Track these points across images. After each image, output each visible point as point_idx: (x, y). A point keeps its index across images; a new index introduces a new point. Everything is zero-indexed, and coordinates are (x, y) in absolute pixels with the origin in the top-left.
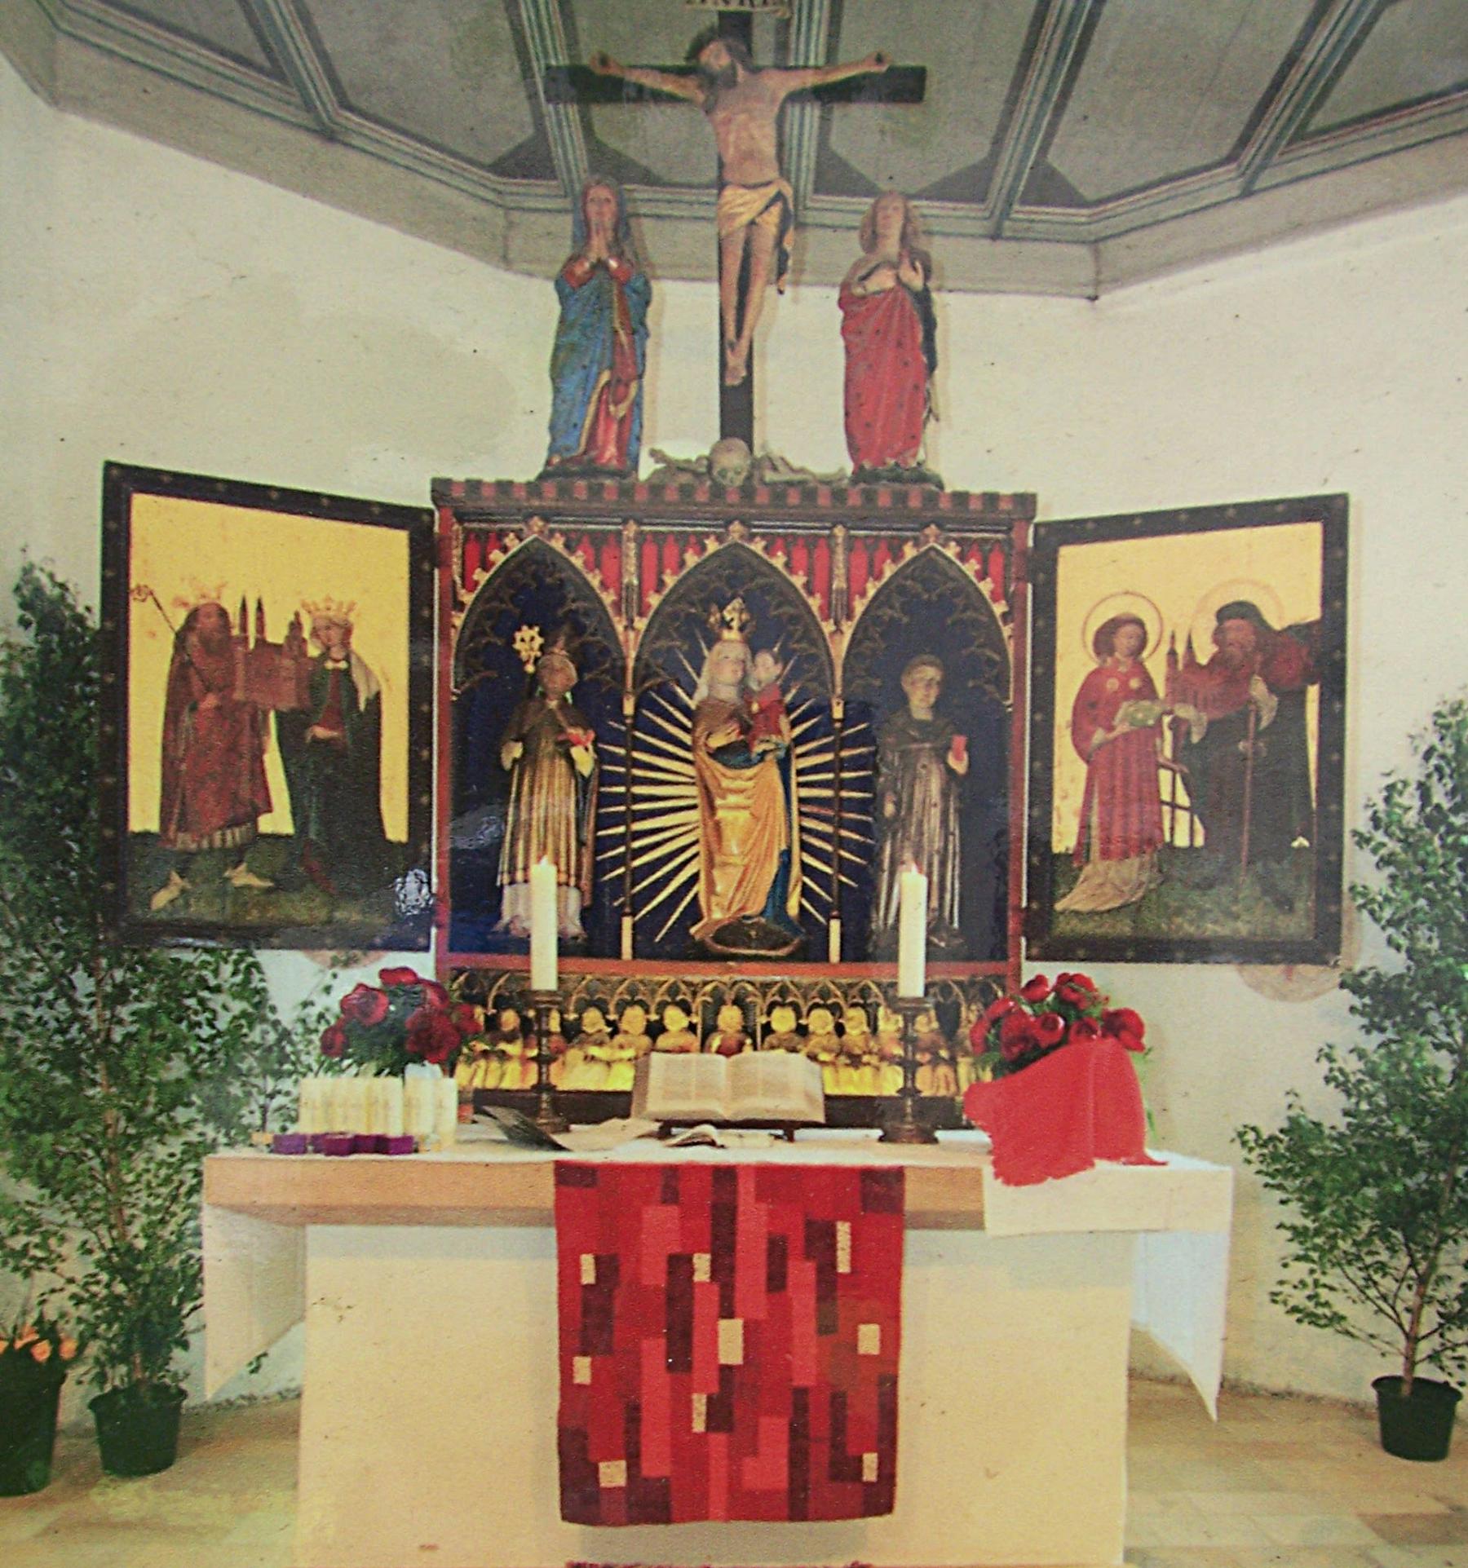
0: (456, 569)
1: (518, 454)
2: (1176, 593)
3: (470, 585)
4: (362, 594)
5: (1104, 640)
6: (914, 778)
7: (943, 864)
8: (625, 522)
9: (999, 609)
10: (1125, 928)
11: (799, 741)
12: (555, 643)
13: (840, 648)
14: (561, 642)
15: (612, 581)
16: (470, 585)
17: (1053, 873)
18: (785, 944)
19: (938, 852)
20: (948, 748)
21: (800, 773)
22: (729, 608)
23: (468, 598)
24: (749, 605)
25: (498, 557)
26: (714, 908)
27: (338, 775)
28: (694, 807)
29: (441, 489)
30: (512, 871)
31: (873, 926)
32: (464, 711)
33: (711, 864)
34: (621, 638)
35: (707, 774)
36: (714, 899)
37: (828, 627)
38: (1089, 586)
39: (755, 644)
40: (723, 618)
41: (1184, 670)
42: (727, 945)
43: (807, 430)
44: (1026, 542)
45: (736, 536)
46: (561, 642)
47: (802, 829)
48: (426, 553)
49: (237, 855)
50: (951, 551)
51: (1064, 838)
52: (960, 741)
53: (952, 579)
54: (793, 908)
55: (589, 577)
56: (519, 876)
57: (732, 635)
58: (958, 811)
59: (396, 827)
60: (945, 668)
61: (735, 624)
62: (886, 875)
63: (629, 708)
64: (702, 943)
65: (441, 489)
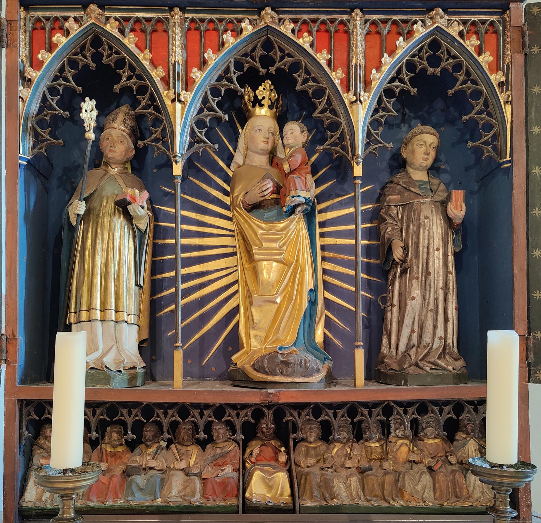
0: (23, 51)
3: (35, 64)
6: (419, 228)
7: (445, 300)
8: (171, 9)
9: (496, 78)
11: (320, 198)
12: (114, 120)
13: (361, 116)
14: (121, 117)
15: (161, 59)
16: (35, 64)
18: (318, 370)
19: (442, 289)
20: (444, 203)
21: (322, 224)
22: (261, 88)
23: (32, 73)
24: (277, 87)
25: (60, 39)
26: (253, 340)
28: (234, 254)
30: (78, 311)
31: (384, 350)
33: (249, 301)
34: (170, 109)
35: (245, 227)
36: (252, 333)
37: (348, 97)
40: (256, 96)
42: (266, 373)
45: (268, 19)
46: (121, 117)
47: (325, 272)
50: (454, 31)
52: (458, 195)
53: (455, 57)
54: (319, 337)
55: (141, 57)
56: (84, 315)
57: (263, 111)
58: (455, 254)
60: (441, 139)
61: (266, 102)
62: (395, 309)
63: (177, 170)
64: (242, 372)
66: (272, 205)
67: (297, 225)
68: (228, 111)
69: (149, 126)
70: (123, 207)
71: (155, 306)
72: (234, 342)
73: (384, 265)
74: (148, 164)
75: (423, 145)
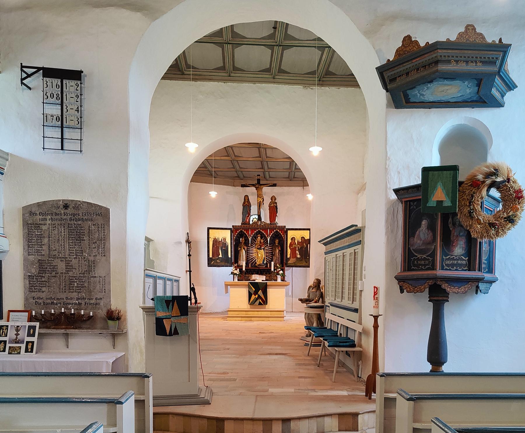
1: (239, 223)
2: (298, 235)
4: (226, 236)
5: (292, 239)
10: (293, 264)
17: (288, 259)
27: (225, 252)
29: (233, 226)
32: (235, 245)
38: (290, 234)
39: (261, 238)
41: (298, 242)
43: (266, 219)
44: (285, 230)
48: (232, 232)
49: (217, 259)
51: (289, 256)
59: (230, 256)
65: (233, 226)
66: (260, 249)
67: (263, 250)
68: (255, 238)
69: (247, 240)
70: (244, 249)
71: (247, 259)
72: (256, 263)
73: (273, 255)
74: (246, 243)
75: (277, 241)
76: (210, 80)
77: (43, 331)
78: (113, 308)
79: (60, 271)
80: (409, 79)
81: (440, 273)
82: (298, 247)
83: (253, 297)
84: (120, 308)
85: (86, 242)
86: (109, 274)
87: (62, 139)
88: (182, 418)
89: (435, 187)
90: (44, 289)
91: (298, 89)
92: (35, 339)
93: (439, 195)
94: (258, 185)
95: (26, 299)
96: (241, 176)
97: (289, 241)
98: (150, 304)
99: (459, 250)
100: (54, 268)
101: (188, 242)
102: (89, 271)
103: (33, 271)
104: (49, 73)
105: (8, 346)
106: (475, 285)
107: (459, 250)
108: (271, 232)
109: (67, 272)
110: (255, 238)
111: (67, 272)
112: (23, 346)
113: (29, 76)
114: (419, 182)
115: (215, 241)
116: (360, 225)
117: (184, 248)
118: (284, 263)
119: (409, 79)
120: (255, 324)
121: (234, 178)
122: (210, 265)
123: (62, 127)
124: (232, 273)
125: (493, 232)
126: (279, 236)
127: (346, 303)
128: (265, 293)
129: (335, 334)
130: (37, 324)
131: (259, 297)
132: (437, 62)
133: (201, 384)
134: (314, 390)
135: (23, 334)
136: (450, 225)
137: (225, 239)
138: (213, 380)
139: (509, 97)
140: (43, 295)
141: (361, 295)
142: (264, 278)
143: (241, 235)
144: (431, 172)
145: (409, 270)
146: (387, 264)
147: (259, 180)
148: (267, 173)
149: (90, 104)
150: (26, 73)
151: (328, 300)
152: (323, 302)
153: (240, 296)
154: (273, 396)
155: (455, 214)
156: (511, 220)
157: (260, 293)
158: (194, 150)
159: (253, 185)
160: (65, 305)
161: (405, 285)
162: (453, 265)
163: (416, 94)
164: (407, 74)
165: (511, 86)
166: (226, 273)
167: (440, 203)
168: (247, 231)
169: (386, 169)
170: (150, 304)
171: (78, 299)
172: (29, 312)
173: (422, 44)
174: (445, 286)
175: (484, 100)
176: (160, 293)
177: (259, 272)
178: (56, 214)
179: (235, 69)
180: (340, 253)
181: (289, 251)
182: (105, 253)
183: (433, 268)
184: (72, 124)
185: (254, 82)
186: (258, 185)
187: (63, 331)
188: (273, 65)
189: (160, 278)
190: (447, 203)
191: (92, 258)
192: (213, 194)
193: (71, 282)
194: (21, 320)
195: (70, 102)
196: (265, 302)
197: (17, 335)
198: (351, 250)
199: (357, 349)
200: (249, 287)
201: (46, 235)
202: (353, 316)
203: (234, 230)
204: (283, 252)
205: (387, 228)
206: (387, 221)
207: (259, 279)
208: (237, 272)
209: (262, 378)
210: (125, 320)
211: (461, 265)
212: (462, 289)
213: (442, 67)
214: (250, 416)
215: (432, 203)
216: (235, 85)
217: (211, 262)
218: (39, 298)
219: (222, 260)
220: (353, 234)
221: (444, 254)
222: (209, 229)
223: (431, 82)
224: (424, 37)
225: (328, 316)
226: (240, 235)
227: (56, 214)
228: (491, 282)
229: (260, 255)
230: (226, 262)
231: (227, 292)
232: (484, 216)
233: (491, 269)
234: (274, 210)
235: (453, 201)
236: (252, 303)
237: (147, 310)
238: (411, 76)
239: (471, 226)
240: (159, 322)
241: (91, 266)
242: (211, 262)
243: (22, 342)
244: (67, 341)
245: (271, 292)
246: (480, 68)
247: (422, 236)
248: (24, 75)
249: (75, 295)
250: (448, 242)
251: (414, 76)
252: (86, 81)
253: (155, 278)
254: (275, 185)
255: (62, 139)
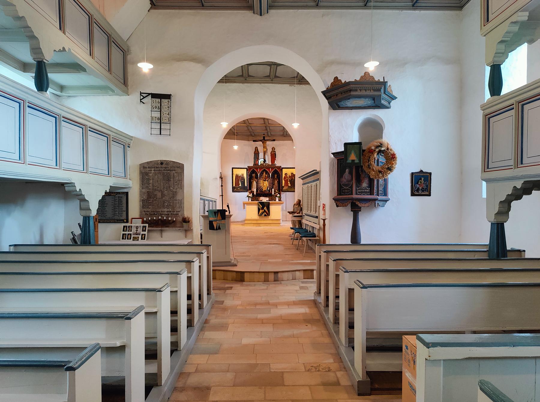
1: (251, 165)
2: (289, 172)
4: (244, 173)
17: (283, 187)
27: (243, 183)
41: (289, 176)
44: (281, 169)
48: (247, 170)
66: (265, 181)
68: (262, 173)
69: (257, 175)
73: (273, 184)
74: (257, 177)
75: (276, 176)
76: (235, 82)
77: (150, 229)
78: (186, 216)
79: (158, 197)
80: (338, 98)
81: (355, 196)
82: (289, 179)
83: (261, 211)
84: (189, 216)
85: (172, 182)
86: (183, 198)
87: (160, 129)
88: (222, 272)
89: (350, 153)
90: (150, 207)
91: (287, 86)
92: (146, 233)
93: (353, 157)
94: (264, 140)
95: (141, 212)
96: (253, 134)
97: (284, 176)
98: (207, 214)
99: (365, 185)
100: (156, 195)
101: (221, 178)
102: (173, 197)
103: (145, 197)
104: (154, 96)
105: (132, 236)
106: (372, 203)
107: (365, 185)
108: (272, 170)
109: (162, 197)
110: (262, 173)
111: (162, 197)
112: (140, 237)
113: (144, 98)
114: (343, 150)
115: (237, 176)
116: (318, 170)
117: (219, 182)
118: (280, 190)
119: (338, 98)
120: (262, 228)
121: (248, 136)
122: (233, 191)
123: (160, 123)
124: (248, 196)
125: (381, 175)
126: (277, 172)
127: (313, 213)
128: (268, 208)
129: (307, 231)
130: (147, 225)
131: (265, 211)
132: (350, 91)
133: (232, 258)
134: (293, 260)
135: (140, 230)
136: (360, 172)
137: (243, 175)
138: (238, 256)
139: (393, 103)
140: (149, 210)
141: (319, 209)
142: (268, 199)
143: (253, 172)
144: (348, 146)
145: (340, 195)
146: (330, 192)
147: (264, 137)
148: (269, 133)
149: (175, 110)
150: (143, 96)
151: (305, 212)
152: (302, 213)
153: (252, 211)
154: (270, 263)
155: (362, 166)
156: (390, 169)
157: (265, 208)
158: (225, 125)
159: (261, 141)
160: (161, 215)
161: (338, 203)
162: (362, 192)
163: (342, 104)
164: (337, 95)
165: (394, 98)
166: (244, 196)
167: (353, 161)
168: (257, 169)
169: (329, 142)
170: (207, 214)
171: (167, 212)
172: (143, 219)
173: (343, 82)
174: (358, 203)
175: (378, 106)
176: (211, 209)
177: (265, 195)
178: (157, 168)
179: (249, 76)
180: (309, 185)
181: (283, 182)
182: (182, 187)
183: (352, 194)
184: (165, 121)
185: (260, 83)
186: (264, 140)
187: (160, 228)
188: (272, 74)
189: (207, 200)
190: (357, 161)
191: (174, 190)
192: (236, 147)
193: (164, 203)
194: (138, 223)
195: (165, 110)
196: (268, 214)
197: (137, 230)
198: (314, 183)
199: (317, 238)
200: (259, 205)
201: (151, 178)
202: (316, 220)
203: (249, 169)
204: (279, 183)
205: (330, 173)
206: (330, 169)
207: (265, 199)
208: (251, 195)
209: (265, 255)
210: (192, 222)
211: (366, 192)
212: (367, 205)
213: (353, 93)
214: (258, 271)
215: (349, 161)
216: (249, 85)
217: (234, 190)
218: (147, 211)
219: (241, 188)
220: (315, 174)
221: (357, 186)
222: (233, 168)
223: (349, 99)
224: (345, 78)
225: (304, 221)
226: (253, 172)
227: (157, 168)
228: (386, 201)
229: (265, 185)
230: (244, 189)
231: (244, 208)
232: (375, 167)
233: (385, 193)
234: (274, 156)
235: (360, 160)
236: (260, 215)
237: (204, 217)
238: (339, 95)
239: (370, 172)
240: (211, 223)
241: (175, 194)
242: (234, 190)
243: (140, 234)
244: (162, 234)
245: (273, 208)
246: (372, 93)
247: (346, 177)
248: (142, 97)
249: (166, 210)
250: (359, 181)
251: (340, 96)
252: (172, 98)
253: (204, 200)
254: (274, 140)
255: (160, 129)
